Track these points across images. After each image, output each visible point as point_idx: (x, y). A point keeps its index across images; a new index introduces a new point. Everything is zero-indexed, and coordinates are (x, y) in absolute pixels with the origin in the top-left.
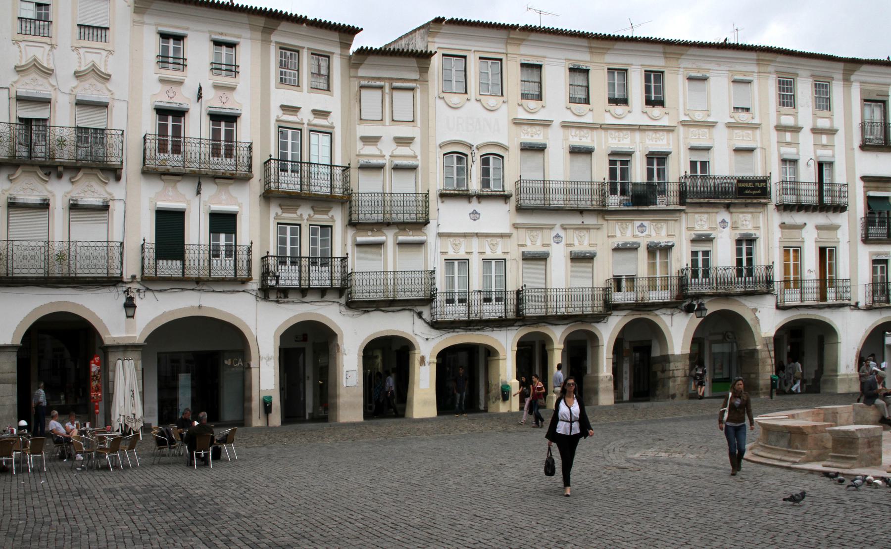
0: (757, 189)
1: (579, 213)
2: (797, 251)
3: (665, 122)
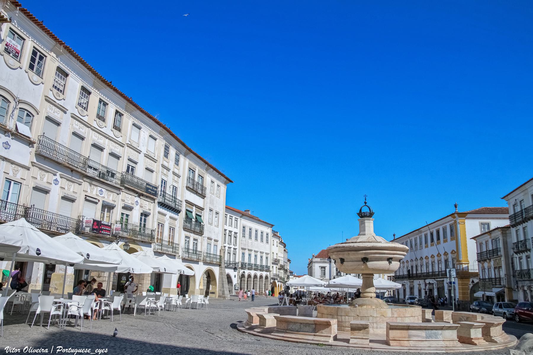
0: (153, 191)
1: (70, 170)
2: (163, 225)
3: (120, 140)
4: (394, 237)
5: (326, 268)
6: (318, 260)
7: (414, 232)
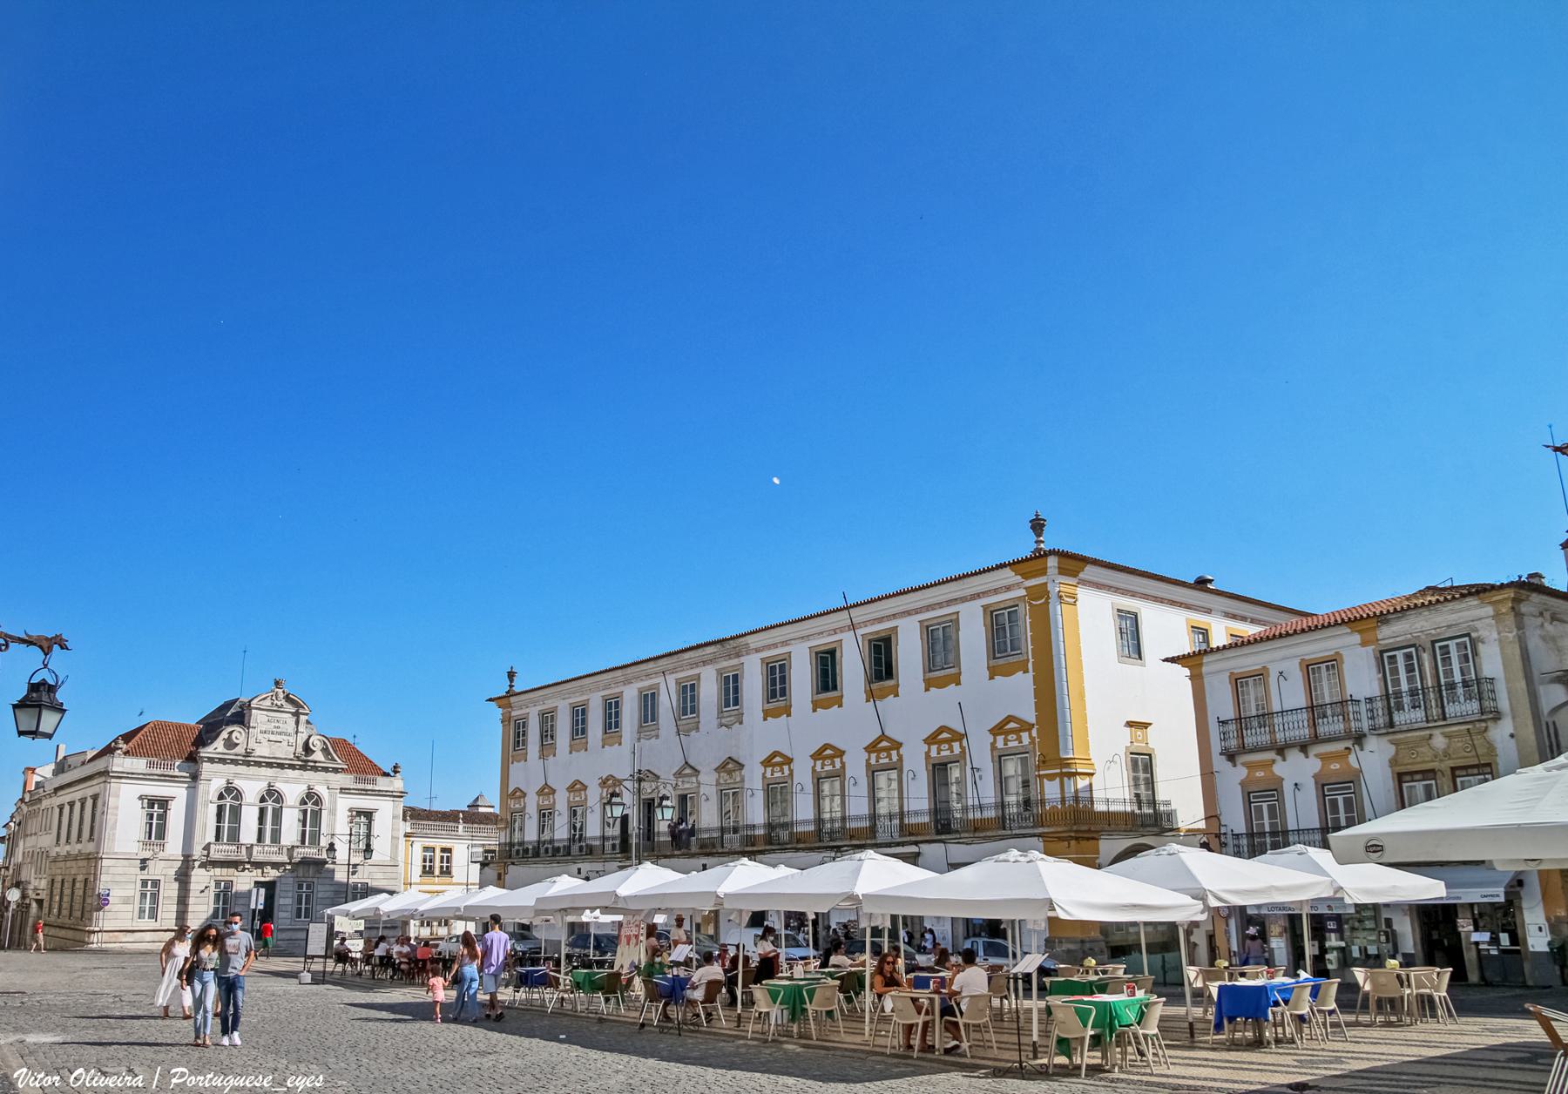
4: (511, 681)
5: (172, 805)
6: (139, 764)
7: (687, 655)
